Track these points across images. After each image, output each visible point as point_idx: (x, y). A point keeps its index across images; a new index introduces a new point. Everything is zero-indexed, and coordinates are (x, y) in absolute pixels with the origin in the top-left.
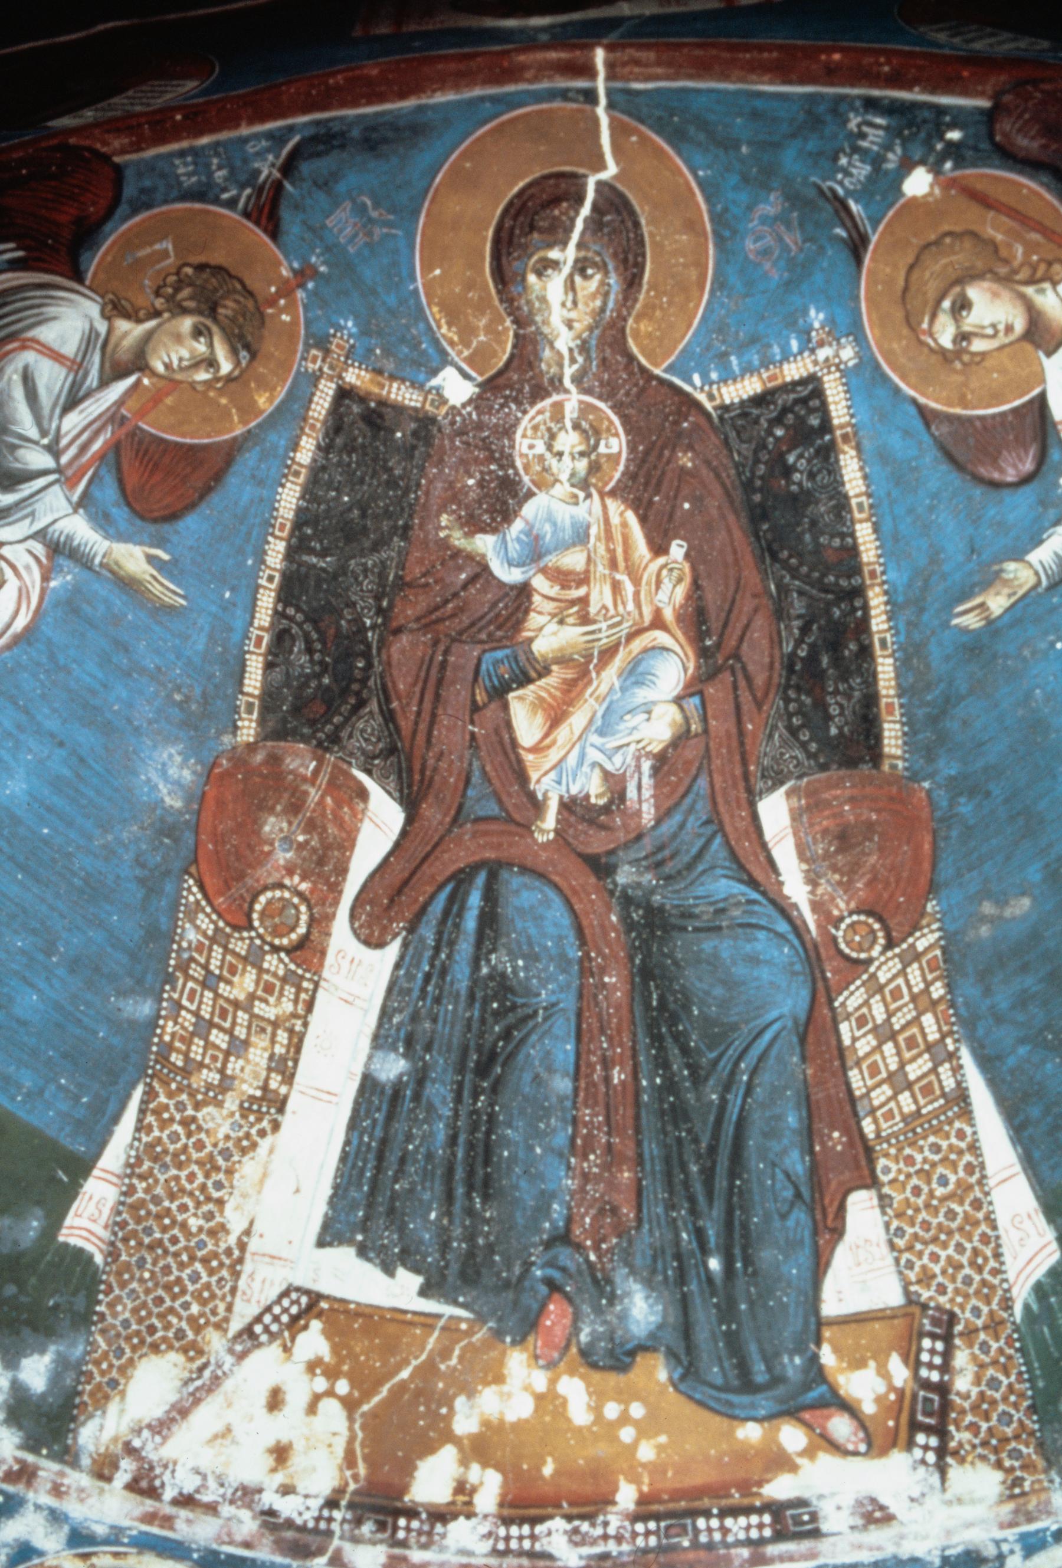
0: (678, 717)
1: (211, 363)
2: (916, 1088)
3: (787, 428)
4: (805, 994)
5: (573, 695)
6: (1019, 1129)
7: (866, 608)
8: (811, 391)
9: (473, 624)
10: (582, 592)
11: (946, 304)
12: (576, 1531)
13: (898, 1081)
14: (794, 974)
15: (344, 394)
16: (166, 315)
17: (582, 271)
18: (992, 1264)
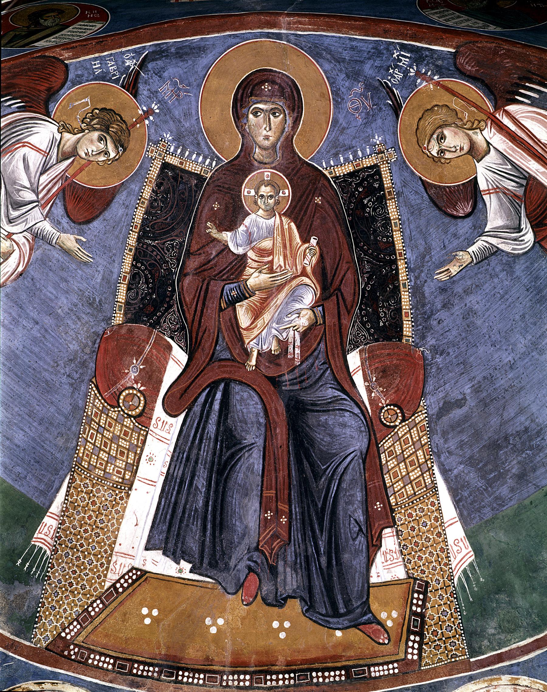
0: (313, 317)
1: (106, 153)
2: (414, 483)
3: (364, 187)
4: (366, 441)
5: (265, 305)
6: (457, 502)
7: (397, 269)
8: (375, 172)
9: (221, 272)
10: (270, 258)
11: (435, 136)
13: (407, 480)
14: (361, 432)
15: (166, 166)
16: (87, 131)
17: (274, 114)
18: (445, 561)
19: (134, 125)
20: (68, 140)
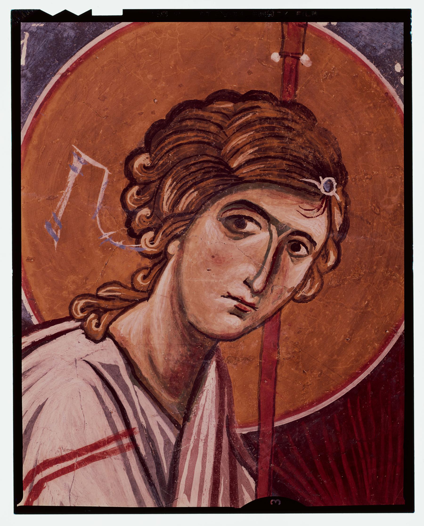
1: (295, 241)
16: (173, 248)
19: (291, 72)
20: (147, 331)
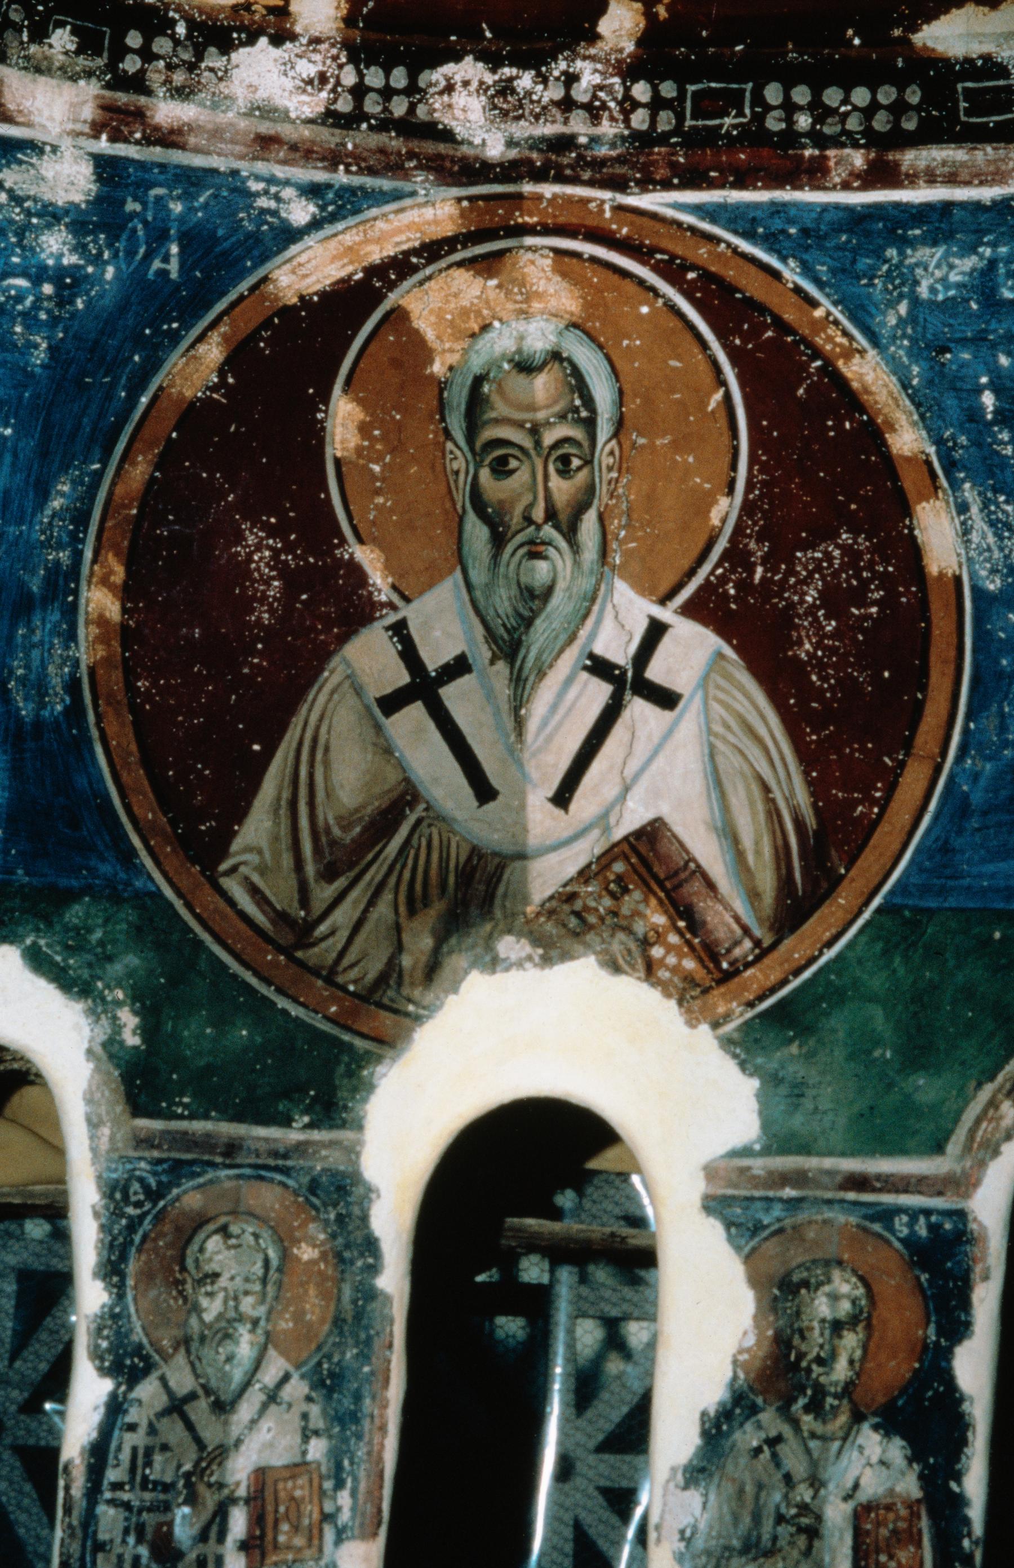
12: (506, 88)
